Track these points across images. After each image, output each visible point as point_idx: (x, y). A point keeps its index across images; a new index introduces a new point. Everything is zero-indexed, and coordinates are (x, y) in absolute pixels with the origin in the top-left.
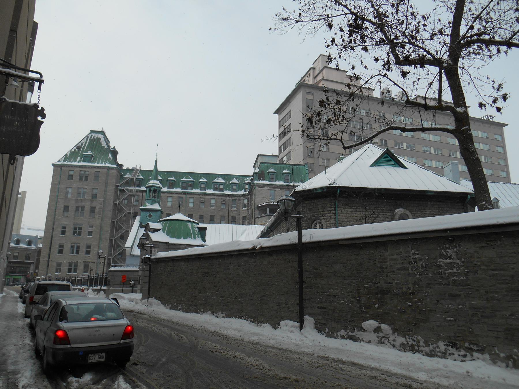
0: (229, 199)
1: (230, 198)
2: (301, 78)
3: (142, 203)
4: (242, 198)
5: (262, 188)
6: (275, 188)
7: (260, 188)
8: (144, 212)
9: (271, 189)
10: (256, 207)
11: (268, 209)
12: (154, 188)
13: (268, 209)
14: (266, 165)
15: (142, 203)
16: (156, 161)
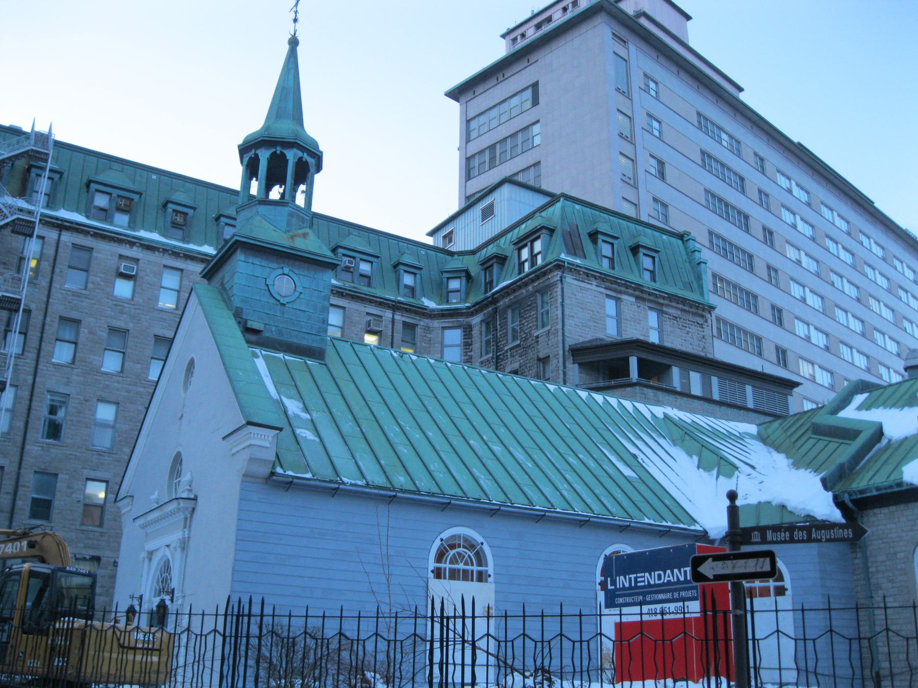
0: (393, 321)
1: (397, 317)
2: (529, 15)
3: (53, 272)
4: (436, 324)
5: (582, 284)
6: (620, 292)
7: (576, 282)
8: (257, 261)
9: (609, 292)
10: (567, 348)
11: (633, 362)
12: (300, 154)
13: (633, 362)
14: (577, 207)
15: (53, 272)
16: (294, 42)
